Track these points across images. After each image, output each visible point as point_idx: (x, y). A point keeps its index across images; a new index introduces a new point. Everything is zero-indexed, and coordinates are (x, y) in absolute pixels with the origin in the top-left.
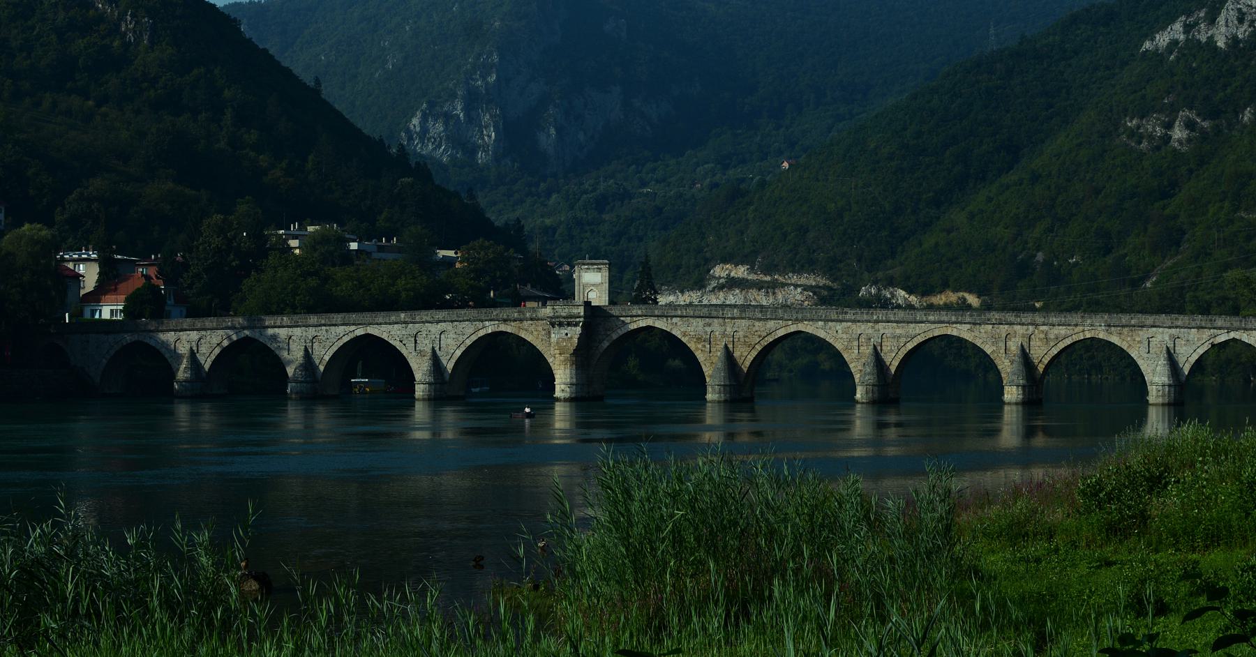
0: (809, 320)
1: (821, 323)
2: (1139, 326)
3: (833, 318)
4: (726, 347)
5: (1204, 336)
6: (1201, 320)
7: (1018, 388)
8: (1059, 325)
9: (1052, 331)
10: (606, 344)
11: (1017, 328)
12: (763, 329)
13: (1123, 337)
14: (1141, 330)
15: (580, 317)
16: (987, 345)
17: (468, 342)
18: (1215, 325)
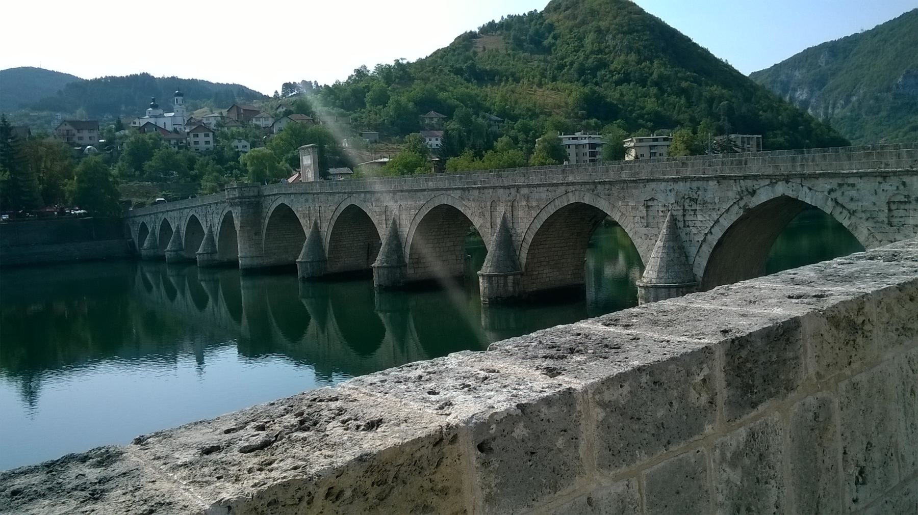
1: (363, 195)
4: (316, 223)
6: (723, 163)
8: (539, 186)
10: (267, 220)
11: (501, 191)
14: (635, 188)
15: (236, 198)
17: (221, 220)
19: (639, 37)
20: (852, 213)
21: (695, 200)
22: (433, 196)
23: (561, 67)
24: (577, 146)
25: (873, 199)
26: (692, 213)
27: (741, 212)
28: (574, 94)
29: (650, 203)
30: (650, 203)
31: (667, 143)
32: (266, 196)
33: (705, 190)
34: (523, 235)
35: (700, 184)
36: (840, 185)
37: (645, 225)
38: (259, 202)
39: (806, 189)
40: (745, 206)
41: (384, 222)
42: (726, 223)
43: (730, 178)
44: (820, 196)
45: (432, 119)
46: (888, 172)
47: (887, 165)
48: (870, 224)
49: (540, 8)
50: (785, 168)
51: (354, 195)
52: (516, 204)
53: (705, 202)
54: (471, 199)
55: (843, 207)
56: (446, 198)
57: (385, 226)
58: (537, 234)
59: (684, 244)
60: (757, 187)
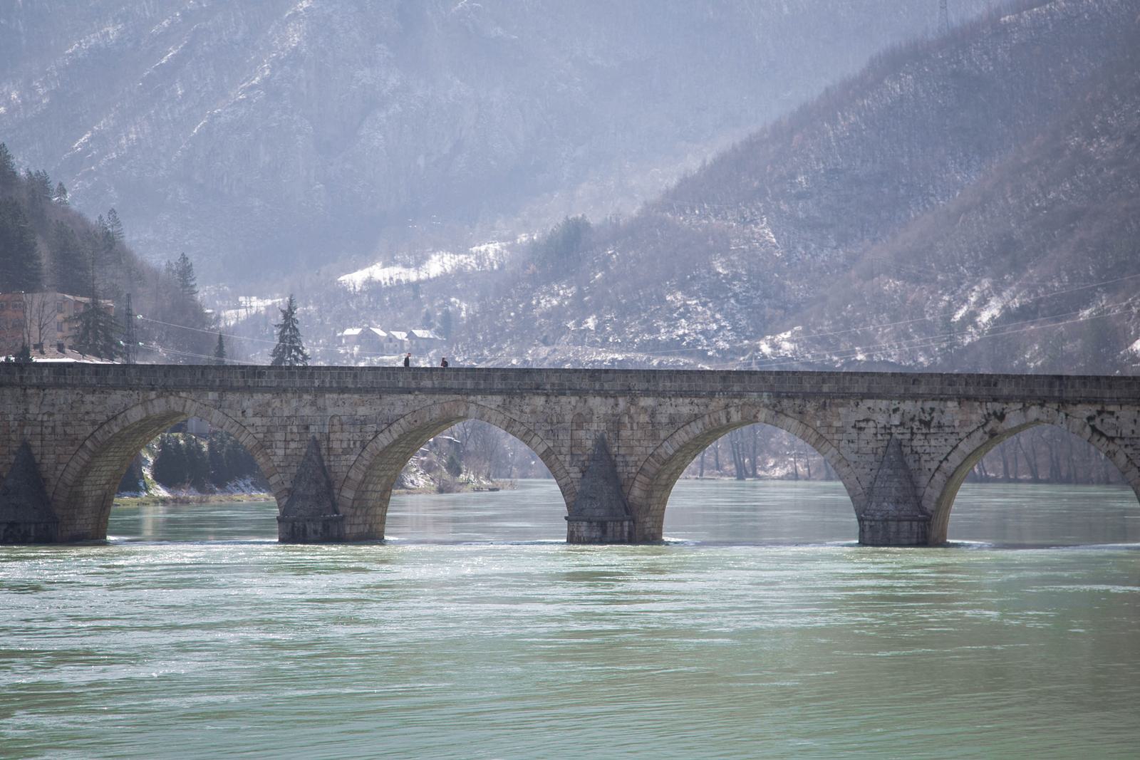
1: (212, 396)
3: (235, 384)
5: (974, 417)
11: (596, 402)
12: (100, 408)
14: (842, 405)
16: (536, 438)
21: (927, 424)
25: (1132, 427)
26: (922, 437)
30: (862, 425)
34: (640, 464)
37: (856, 450)
41: (280, 444)
48: (1129, 450)
51: (183, 394)
52: (626, 419)
53: (940, 426)
54: (528, 410)
55: (1102, 434)
57: (281, 452)
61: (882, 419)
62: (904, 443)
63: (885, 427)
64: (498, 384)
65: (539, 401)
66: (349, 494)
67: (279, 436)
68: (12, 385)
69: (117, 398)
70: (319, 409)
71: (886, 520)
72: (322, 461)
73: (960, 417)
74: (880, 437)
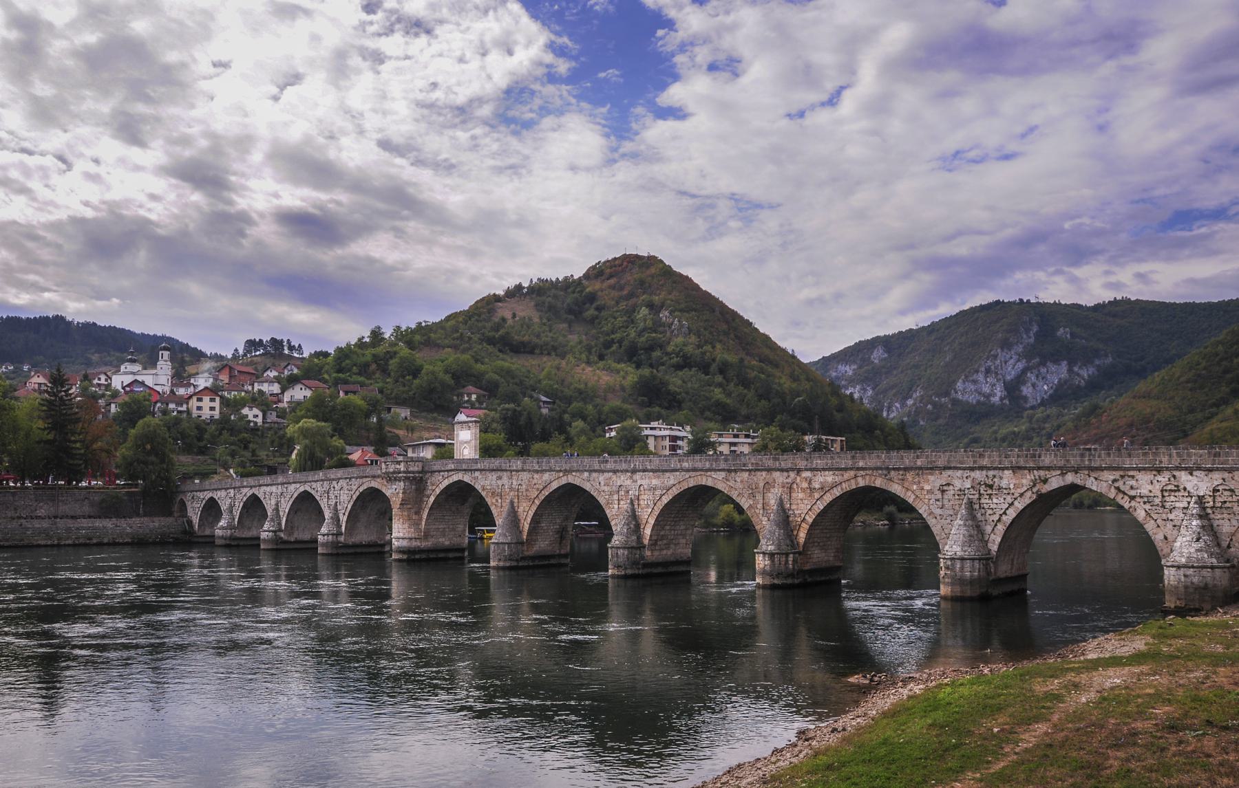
0: (578, 471)
1: (586, 474)
2: (927, 469)
4: (512, 503)
6: (1018, 456)
7: (764, 557)
8: (824, 470)
9: (816, 479)
10: (432, 499)
11: (778, 472)
12: (540, 482)
13: (906, 485)
14: (932, 474)
15: (400, 473)
17: (355, 497)
18: (1041, 465)
19: (698, 317)
20: (1132, 498)
21: (991, 487)
22: (687, 476)
23: (608, 345)
24: (656, 437)
25: (1150, 487)
26: (987, 497)
27: (1035, 496)
28: (629, 378)
29: (945, 488)
30: (945, 488)
31: (749, 440)
32: (435, 472)
33: (1001, 478)
35: (995, 473)
36: (1122, 477)
38: (421, 478)
39: (1092, 479)
40: (1038, 491)
41: (616, 502)
42: (1020, 505)
43: (1025, 468)
44: (1105, 484)
45: (469, 395)
46: (1163, 467)
47: (1161, 462)
48: (1147, 507)
49: (578, 273)
50: (1074, 461)
51: (574, 474)
52: (795, 486)
53: (1000, 488)
55: (1124, 493)
56: (704, 479)
57: (616, 506)
58: (819, 515)
59: (980, 523)
60: (1049, 476)
61: (958, 484)
62: (974, 501)
63: (960, 490)
64: (723, 465)
65: (746, 475)
66: (648, 531)
67: (616, 497)
68: (506, 470)
69: (546, 476)
70: (634, 481)
71: (953, 559)
72: (633, 511)
73: (1014, 481)
74: (957, 497)
